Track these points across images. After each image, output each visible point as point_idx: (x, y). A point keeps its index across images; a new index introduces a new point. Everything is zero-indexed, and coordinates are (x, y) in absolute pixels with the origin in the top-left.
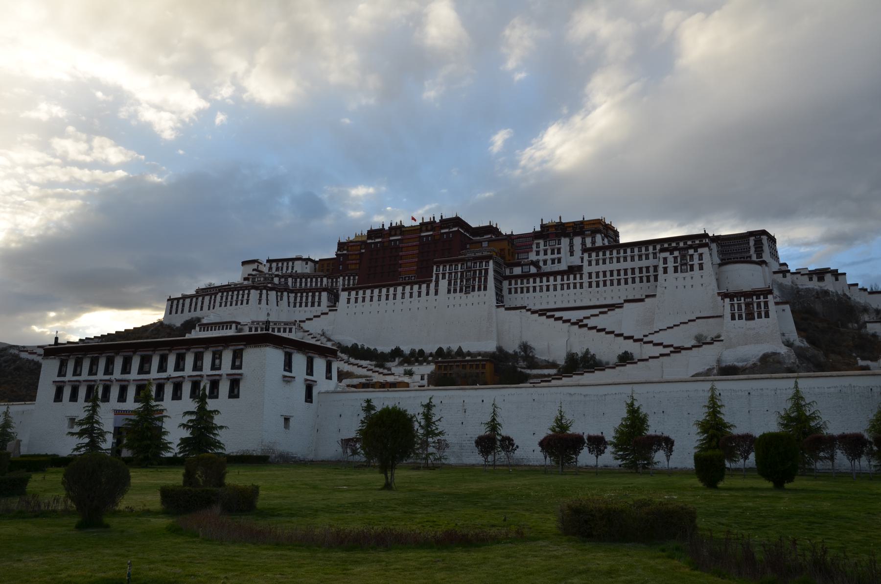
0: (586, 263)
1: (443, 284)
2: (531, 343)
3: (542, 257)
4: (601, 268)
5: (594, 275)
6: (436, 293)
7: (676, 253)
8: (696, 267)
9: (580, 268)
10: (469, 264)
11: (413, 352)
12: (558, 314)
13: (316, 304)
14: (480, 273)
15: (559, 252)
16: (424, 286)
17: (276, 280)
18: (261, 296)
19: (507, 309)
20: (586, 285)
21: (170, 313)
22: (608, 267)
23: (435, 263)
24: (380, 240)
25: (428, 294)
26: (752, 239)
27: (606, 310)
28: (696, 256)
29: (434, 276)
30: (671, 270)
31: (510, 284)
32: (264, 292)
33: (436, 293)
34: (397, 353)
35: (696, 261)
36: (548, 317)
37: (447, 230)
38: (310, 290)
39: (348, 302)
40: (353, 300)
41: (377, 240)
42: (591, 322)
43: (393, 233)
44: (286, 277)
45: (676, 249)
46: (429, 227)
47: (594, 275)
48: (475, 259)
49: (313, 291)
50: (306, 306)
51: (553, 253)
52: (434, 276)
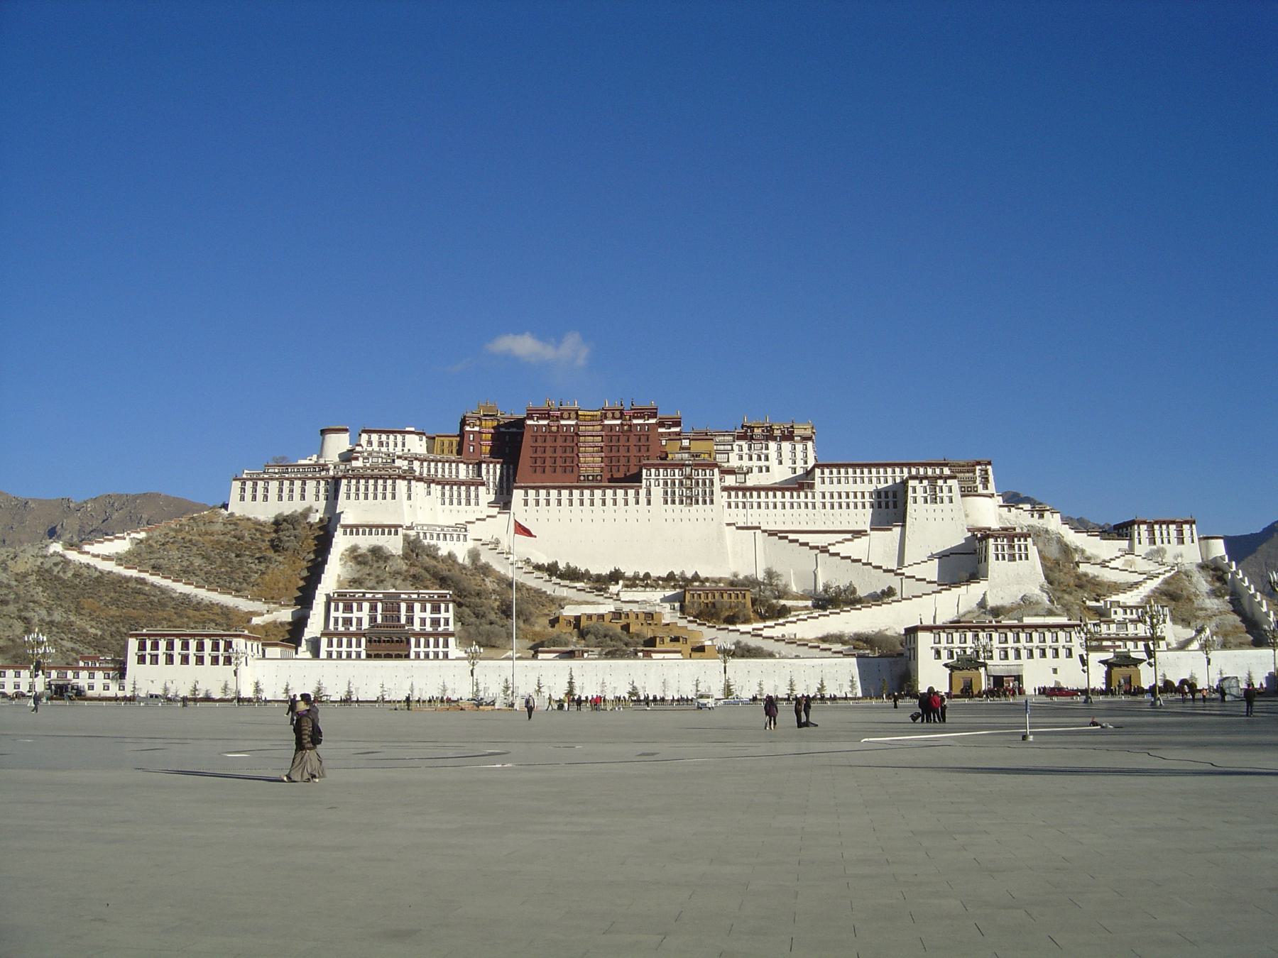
0: (817, 481)
1: (657, 492)
2: (776, 569)
3: (746, 463)
4: (835, 488)
5: (828, 495)
6: (649, 503)
7: (925, 482)
8: (946, 500)
9: (811, 486)
10: (688, 469)
11: (636, 577)
12: (803, 538)
13: (473, 502)
14: (704, 483)
15: (767, 459)
16: (631, 492)
17: (398, 463)
18: (409, 489)
19: (738, 528)
20: (819, 505)
21: (242, 498)
22: (843, 488)
23: (645, 465)
24: (545, 422)
26: (978, 468)
27: (849, 536)
28: (945, 489)
30: (920, 500)
31: (729, 496)
32: (413, 482)
33: (649, 503)
34: (615, 576)
35: (946, 493)
36: (791, 541)
37: (641, 421)
38: (463, 483)
40: (531, 502)
41: (542, 422)
42: (844, 549)
43: (566, 415)
44: (411, 459)
45: (926, 478)
47: (828, 495)
48: (696, 466)
49: (468, 484)
50: (460, 503)
51: (759, 458)
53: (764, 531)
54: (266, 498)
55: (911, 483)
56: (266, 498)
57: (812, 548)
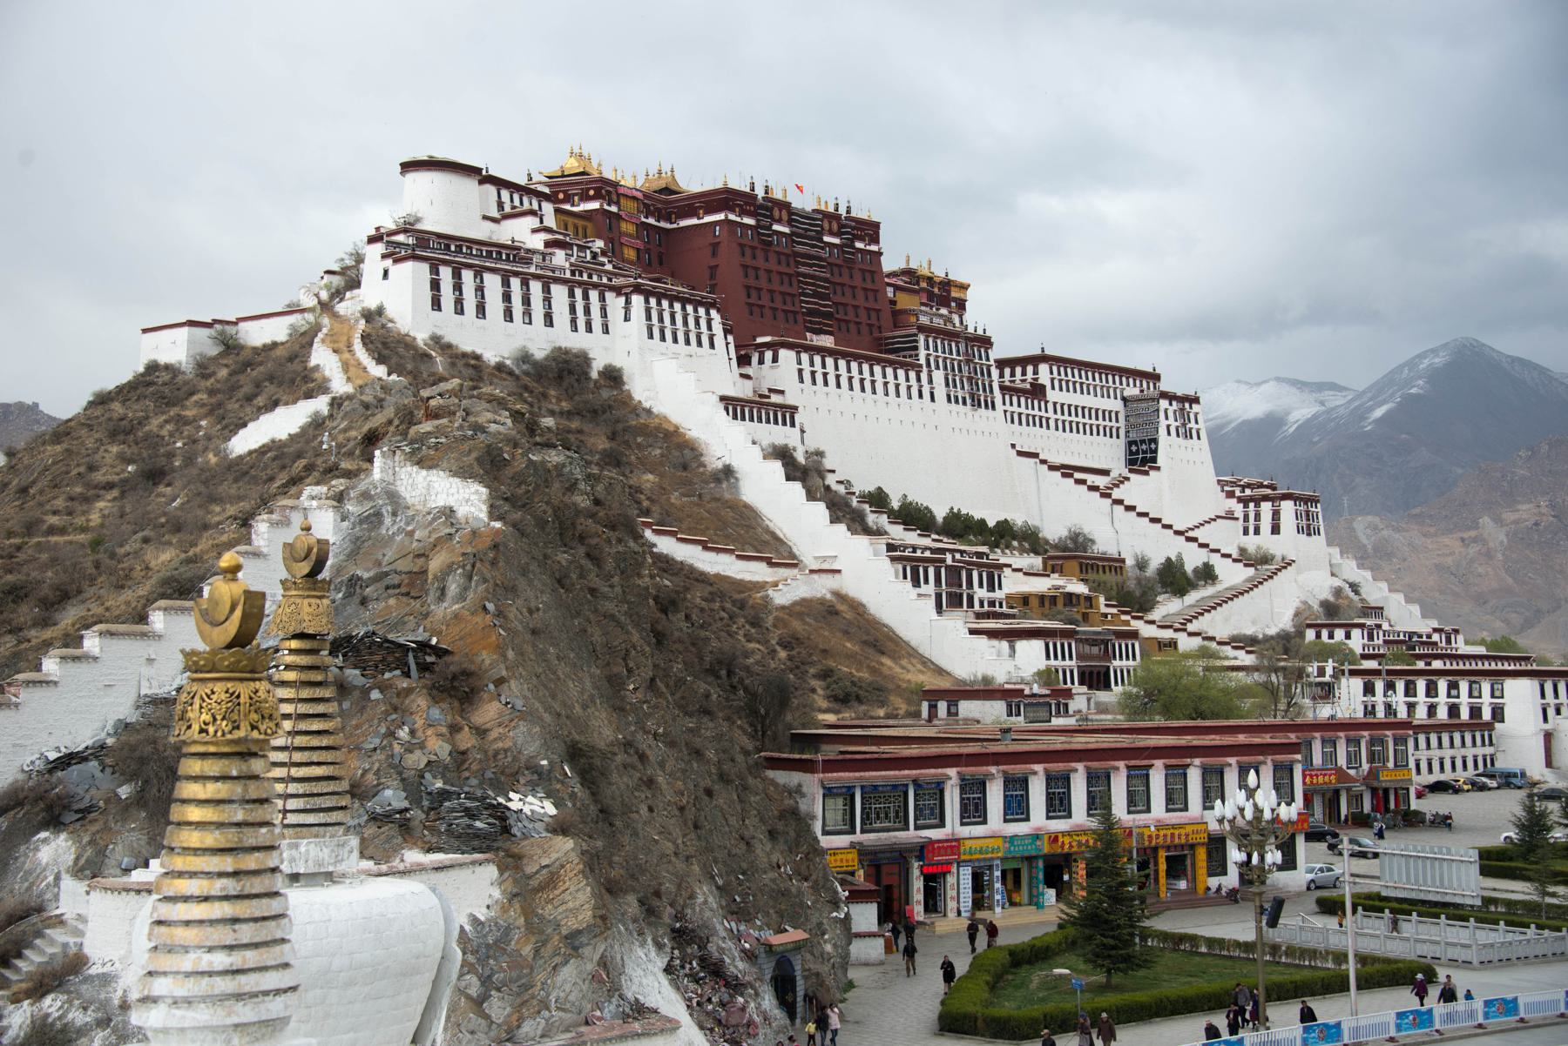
1: (939, 376)
6: (933, 399)
12: (1092, 479)
16: (912, 375)
19: (1020, 453)
21: (436, 304)
25: (921, 396)
29: (922, 361)
33: (933, 399)
36: (1078, 482)
39: (802, 381)
40: (807, 376)
41: (750, 221)
43: (776, 214)
46: (835, 227)
52: (922, 361)
53: (1043, 462)
54: (481, 310)
55: (1164, 404)
56: (481, 310)
57: (1104, 495)
